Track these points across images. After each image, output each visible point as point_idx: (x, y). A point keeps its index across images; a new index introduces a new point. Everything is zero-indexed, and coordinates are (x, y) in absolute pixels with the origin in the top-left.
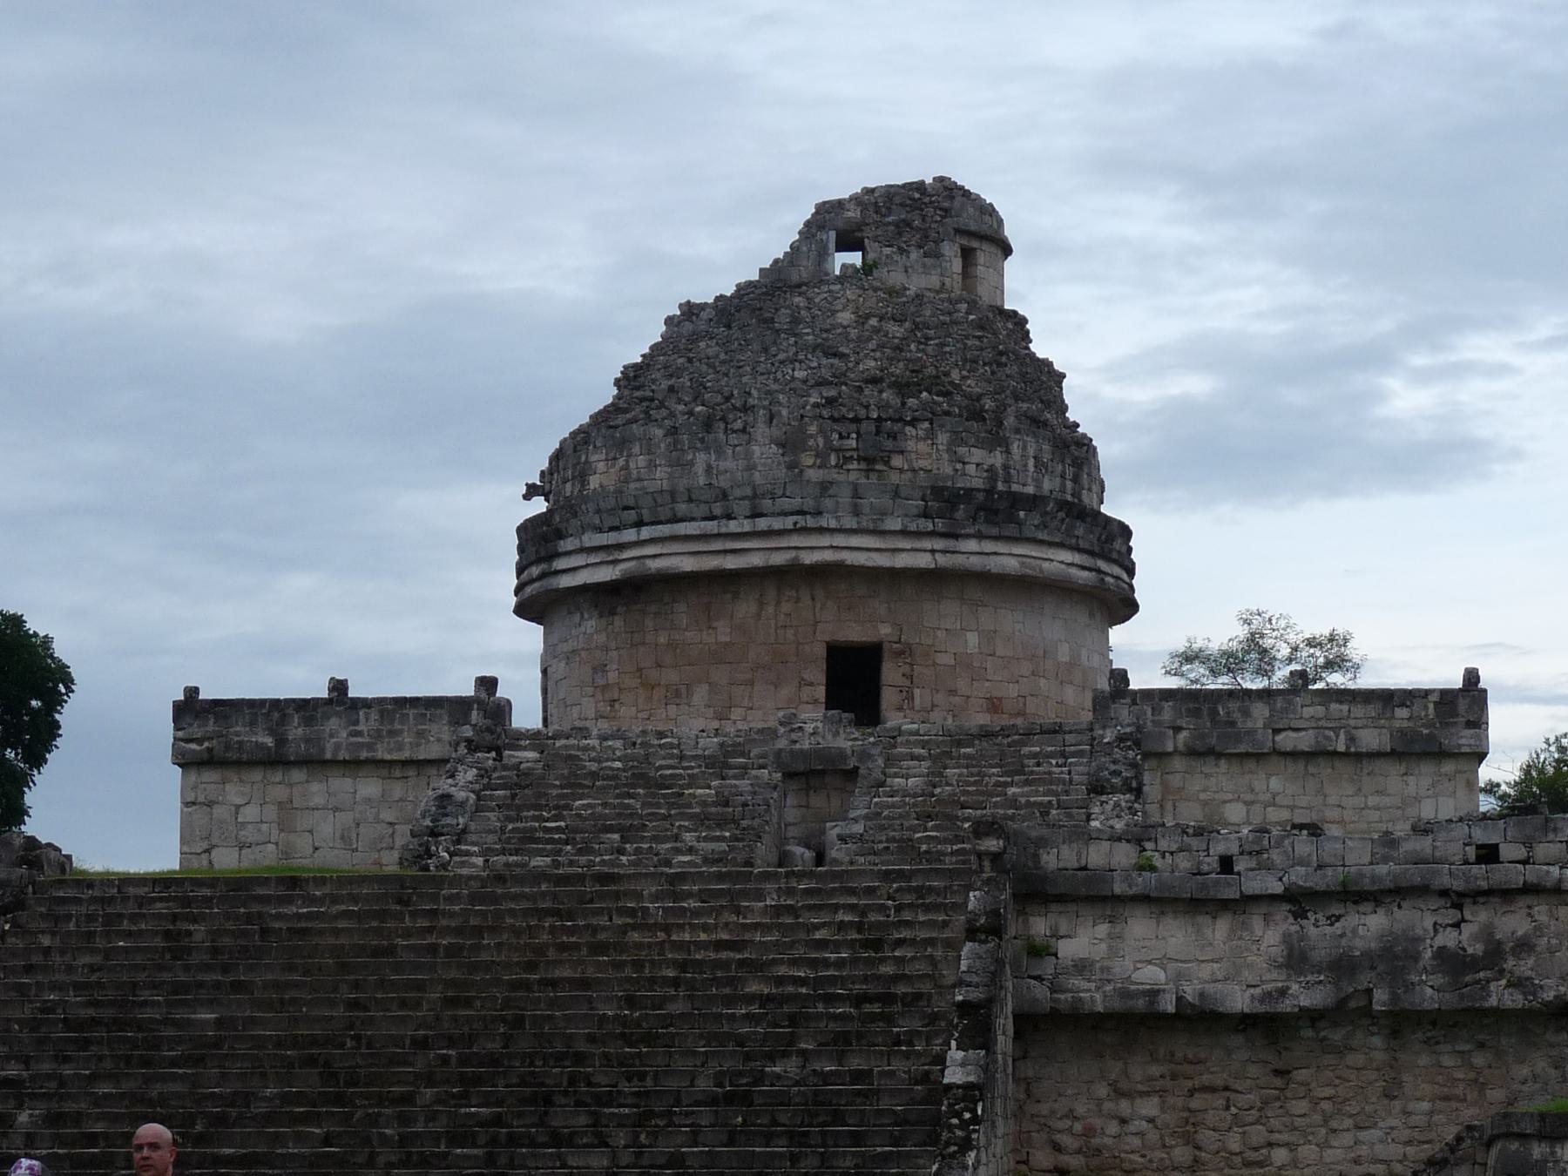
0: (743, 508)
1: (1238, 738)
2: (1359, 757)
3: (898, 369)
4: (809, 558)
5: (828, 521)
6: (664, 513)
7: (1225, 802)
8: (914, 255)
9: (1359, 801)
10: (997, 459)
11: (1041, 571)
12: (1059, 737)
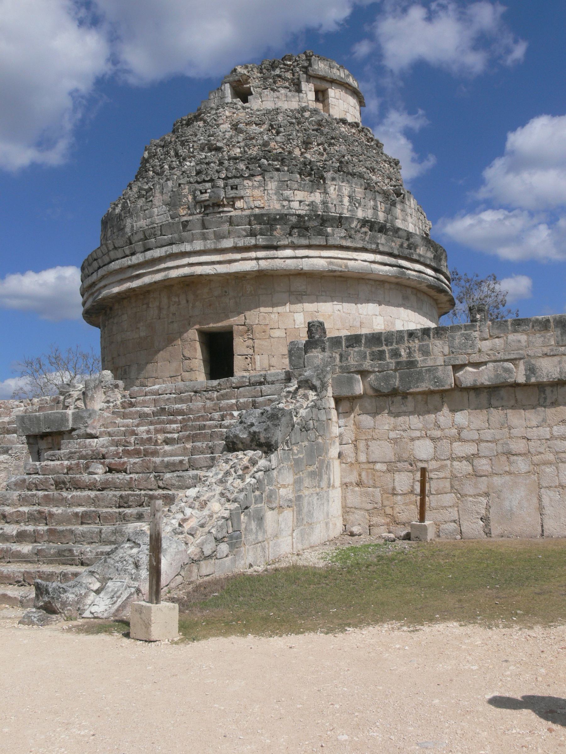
0: (139, 246)
1: (420, 378)
2: (541, 387)
3: (254, 152)
4: (174, 274)
5: (187, 247)
6: (106, 259)
7: (412, 440)
8: (283, 91)
9: (545, 432)
10: (317, 197)
11: (346, 266)
12: (258, 388)
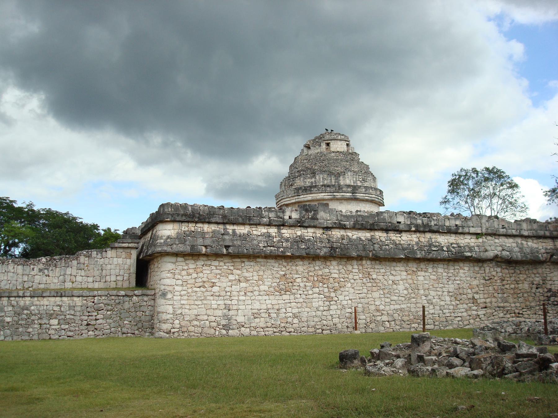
10: (313, 180)
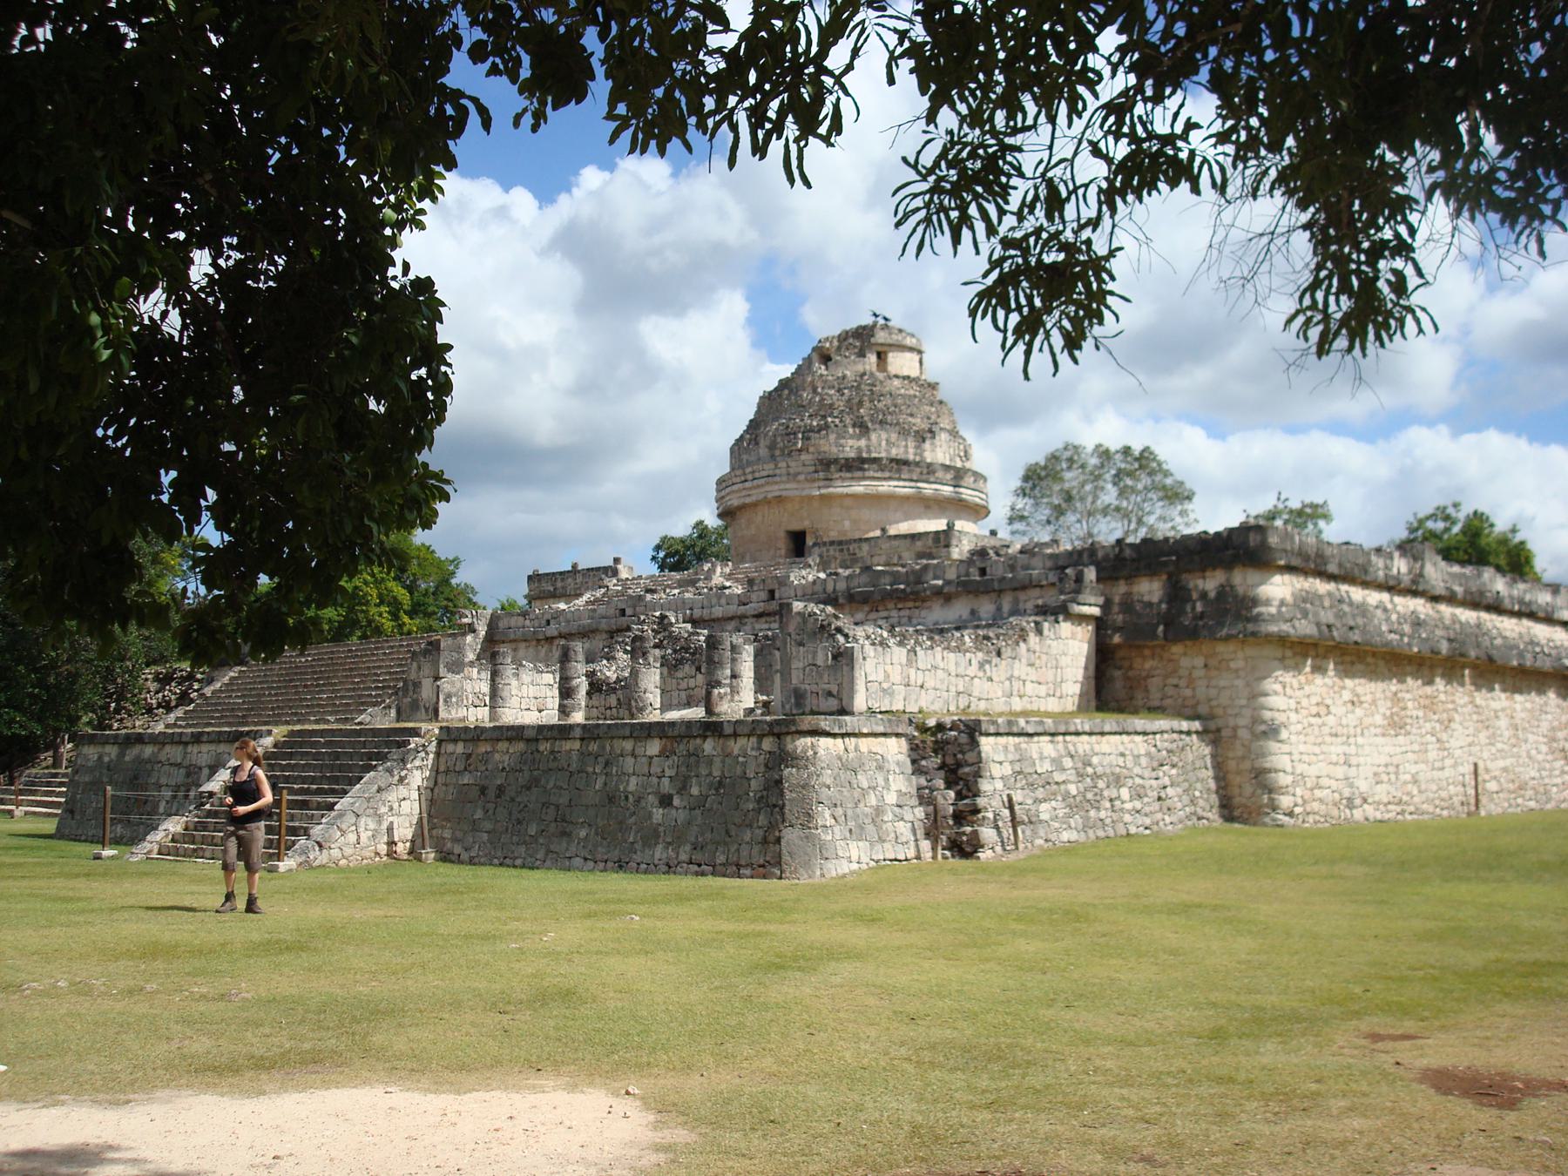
0: (750, 477)
10: (863, 443)
